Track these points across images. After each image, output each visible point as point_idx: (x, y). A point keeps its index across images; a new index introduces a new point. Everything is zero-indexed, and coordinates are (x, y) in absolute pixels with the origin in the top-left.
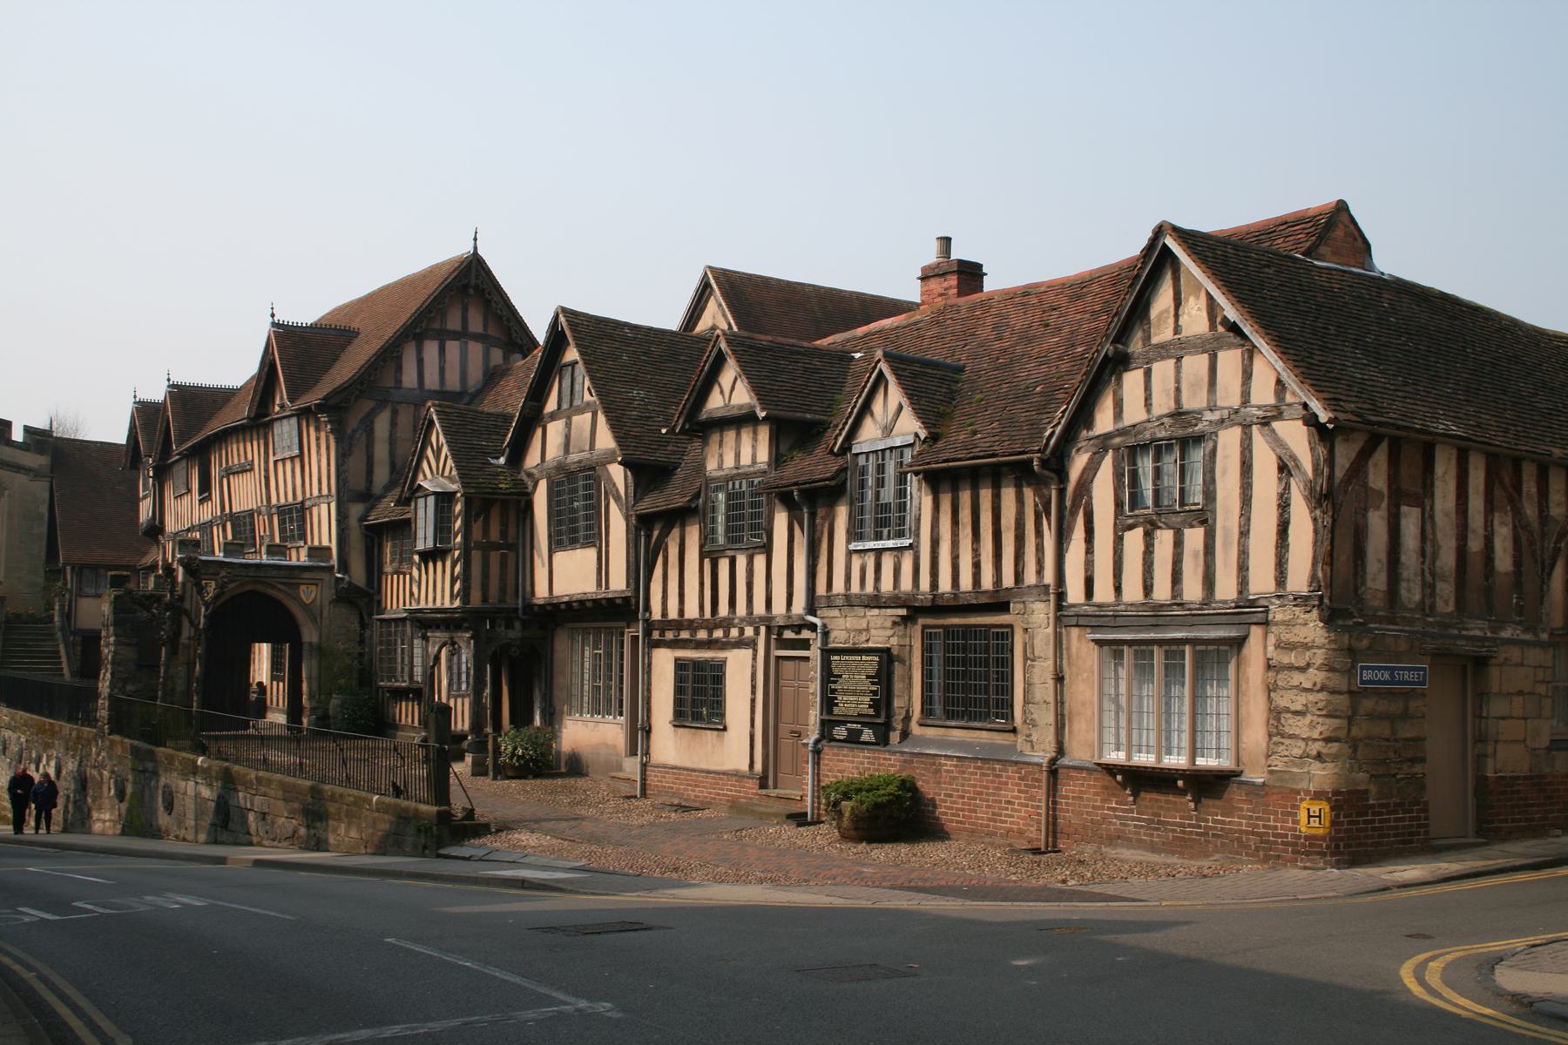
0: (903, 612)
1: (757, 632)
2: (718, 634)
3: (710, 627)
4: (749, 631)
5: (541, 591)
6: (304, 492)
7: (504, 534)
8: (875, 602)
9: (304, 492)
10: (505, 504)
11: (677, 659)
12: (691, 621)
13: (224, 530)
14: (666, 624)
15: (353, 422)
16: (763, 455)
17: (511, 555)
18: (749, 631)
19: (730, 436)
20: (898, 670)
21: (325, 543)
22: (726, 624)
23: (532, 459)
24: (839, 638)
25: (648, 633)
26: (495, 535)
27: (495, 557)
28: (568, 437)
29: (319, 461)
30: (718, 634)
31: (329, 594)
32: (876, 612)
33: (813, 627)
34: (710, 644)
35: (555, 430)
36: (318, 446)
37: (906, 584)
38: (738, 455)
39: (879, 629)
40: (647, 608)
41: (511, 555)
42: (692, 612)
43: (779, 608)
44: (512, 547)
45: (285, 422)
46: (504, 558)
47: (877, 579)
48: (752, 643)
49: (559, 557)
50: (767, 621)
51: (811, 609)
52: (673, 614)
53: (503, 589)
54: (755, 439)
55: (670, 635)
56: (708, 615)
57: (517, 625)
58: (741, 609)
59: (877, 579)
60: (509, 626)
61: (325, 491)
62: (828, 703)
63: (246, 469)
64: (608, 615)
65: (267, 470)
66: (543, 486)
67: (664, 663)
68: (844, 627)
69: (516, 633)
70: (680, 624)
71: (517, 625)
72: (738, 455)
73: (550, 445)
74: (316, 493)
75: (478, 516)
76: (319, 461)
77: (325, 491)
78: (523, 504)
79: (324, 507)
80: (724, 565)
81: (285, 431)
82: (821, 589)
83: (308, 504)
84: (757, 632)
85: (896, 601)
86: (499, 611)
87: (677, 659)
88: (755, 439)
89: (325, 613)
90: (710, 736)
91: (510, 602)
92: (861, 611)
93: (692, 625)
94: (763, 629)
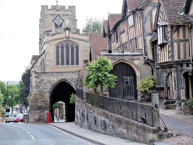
6: (136, 35)
7: (184, 36)
9: (136, 35)
10: (184, 26)
13: (121, 49)
15: (146, 13)
21: (141, 48)
26: (181, 37)
27: (182, 44)
29: (138, 25)
31: (143, 62)
36: (138, 22)
41: (187, 43)
44: (187, 41)
45: (130, 16)
46: (185, 44)
53: (185, 55)
57: (190, 65)
60: (188, 66)
61: (140, 34)
63: (124, 32)
65: (128, 31)
71: (190, 65)
74: (138, 35)
75: (175, 31)
76: (138, 25)
77: (140, 34)
78: (190, 26)
79: (140, 38)
81: (131, 19)
83: (137, 38)
86: (184, 61)
89: (142, 67)
91: (188, 58)
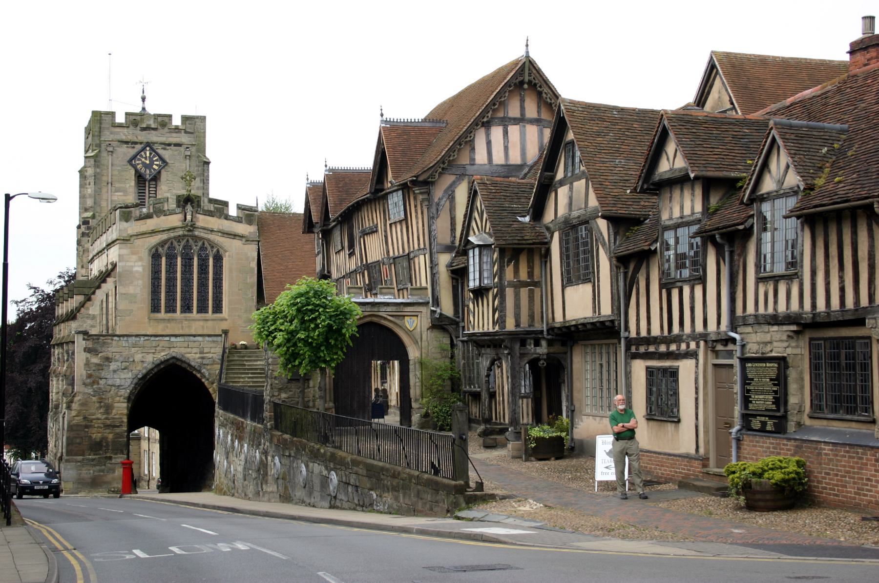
0: (794, 328)
1: (698, 346)
2: (673, 347)
3: (668, 341)
4: (693, 345)
5: (559, 318)
7: (531, 274)
8: (775, 320)
11: (647, 368)
12: (656, 338)
14: (640, 341)
16: (698, 208)
17: (537, 291)
18: (693, 345)
19: (677, 193)
20: (792, 374)
22: (678, 339)
23: (549, 216)
24: (753, 350)
25: (628, 348)
28: (571, 198)
30: (673, 347)
32: (775, 328)
33: (734, 340)
34: (669, 355)
35: (563, 192)
37: (795, 306)
38: (682, 208)
39: (776, 342)
40: (627, 328)
41: (537, 291)
42: (656, 331)
43: (712, 327)
44: (537, 284)
46: (531, 292)
47: (776, 302)
48: (693, 355)
49: (569, 290)
50: (704, 336)
51: (733, 327)
52: (644, 333)
53: (532, 317)
54: (693, 195)
55: (642, 349)
56: (666, 333)
57: (544, 343)
58: (687, 329)
59: (776, 302)
60: (537, 344)
62: (746, 401)
64: (601, 333)
66: (556, 235)
67: (639, 368)
68: (755, 340)
69: (543, 349)
70: (649, 340)
71: (544, 343)
72: (682, 208)
73: (561, 204)
80: (675, 293)
82: (739, 312)
84: (698, 346)
85: (789, 319)
87: (647, 368)
88: (693, 195)
90: (670, 427)
91: (538, 327)
92: (766, 328)
93: (655, 341)
94: (702, 343)
